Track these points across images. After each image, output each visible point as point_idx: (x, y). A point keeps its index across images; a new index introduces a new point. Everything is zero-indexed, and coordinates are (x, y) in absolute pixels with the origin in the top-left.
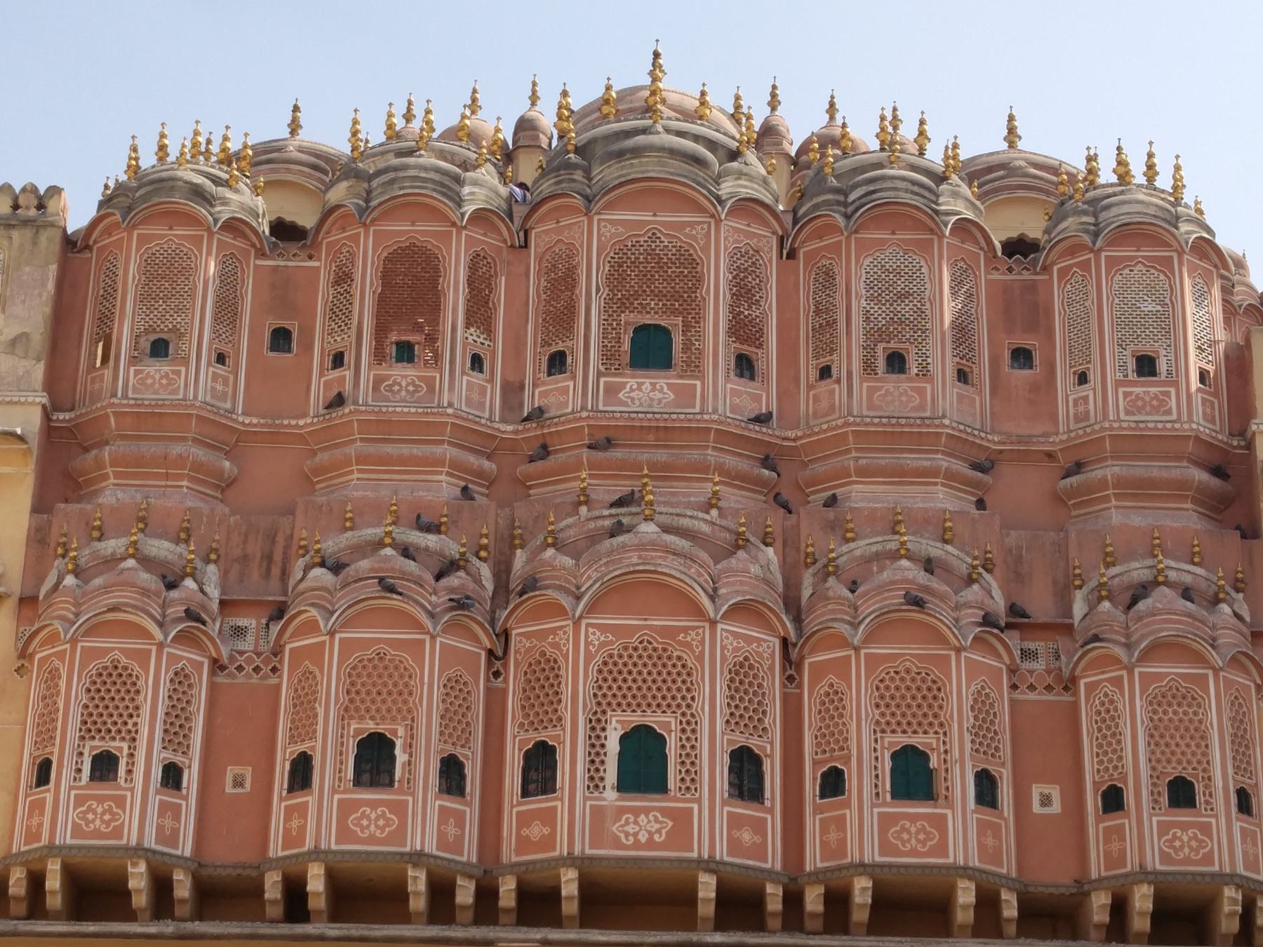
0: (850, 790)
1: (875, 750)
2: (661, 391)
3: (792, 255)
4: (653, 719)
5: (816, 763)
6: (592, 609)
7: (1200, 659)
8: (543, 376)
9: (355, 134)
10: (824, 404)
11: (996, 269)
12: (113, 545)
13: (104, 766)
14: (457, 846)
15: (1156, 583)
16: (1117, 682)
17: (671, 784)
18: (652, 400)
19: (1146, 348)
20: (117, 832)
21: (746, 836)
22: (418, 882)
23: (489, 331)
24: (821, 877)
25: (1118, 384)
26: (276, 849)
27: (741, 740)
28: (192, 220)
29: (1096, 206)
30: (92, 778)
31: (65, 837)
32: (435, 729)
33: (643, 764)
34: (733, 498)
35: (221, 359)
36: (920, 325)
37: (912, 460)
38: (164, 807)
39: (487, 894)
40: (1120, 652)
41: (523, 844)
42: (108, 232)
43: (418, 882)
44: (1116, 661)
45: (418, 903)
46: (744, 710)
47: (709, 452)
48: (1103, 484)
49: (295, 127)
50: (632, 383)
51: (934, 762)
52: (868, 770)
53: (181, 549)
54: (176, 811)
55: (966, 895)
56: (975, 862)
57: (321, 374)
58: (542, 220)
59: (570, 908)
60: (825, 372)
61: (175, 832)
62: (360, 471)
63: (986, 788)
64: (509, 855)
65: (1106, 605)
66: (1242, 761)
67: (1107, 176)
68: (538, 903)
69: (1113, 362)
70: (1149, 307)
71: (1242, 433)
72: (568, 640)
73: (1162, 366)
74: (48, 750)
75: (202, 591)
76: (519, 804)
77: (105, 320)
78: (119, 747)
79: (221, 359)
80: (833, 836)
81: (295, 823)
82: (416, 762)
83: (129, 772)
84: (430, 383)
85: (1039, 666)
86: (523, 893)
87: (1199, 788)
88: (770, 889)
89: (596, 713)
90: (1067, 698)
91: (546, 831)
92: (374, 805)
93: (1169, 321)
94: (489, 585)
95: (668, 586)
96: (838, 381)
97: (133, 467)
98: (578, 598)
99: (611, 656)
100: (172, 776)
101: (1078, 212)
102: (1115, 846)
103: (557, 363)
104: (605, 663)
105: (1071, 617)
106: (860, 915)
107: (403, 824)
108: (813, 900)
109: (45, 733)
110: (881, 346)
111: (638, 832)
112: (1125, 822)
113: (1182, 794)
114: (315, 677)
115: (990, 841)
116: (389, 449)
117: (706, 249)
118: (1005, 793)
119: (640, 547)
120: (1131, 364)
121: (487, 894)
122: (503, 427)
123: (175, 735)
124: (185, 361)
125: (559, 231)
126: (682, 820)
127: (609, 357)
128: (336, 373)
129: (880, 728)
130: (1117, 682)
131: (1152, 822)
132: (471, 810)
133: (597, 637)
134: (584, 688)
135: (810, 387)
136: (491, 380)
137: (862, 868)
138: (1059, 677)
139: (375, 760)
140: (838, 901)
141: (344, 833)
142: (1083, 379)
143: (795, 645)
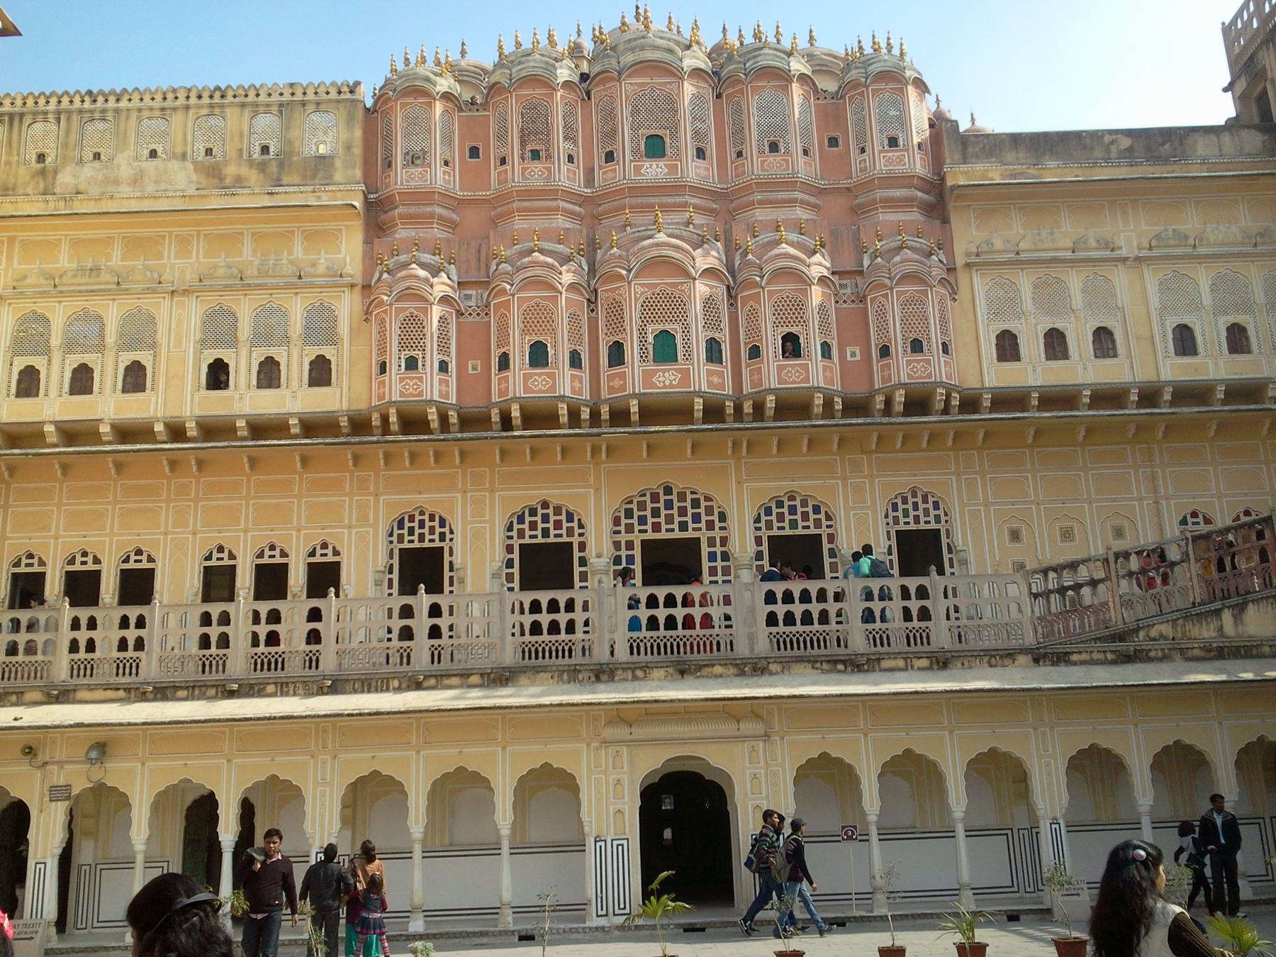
3: (719, 96)
4: (668, 327)
6: (636, 277)
7: (924, 282)
8: (603, 164)
9: (500, 47)
12: (403, 258)
13: (412, 364)
14: (580, 392)
15: (901, 248)
16: (886, 296)
19: (893, 133)
20: (421, 394)
21: (715, 380)
22: (563, 410)
23: (575, 143)
25: (880, 152)
27: (710, 334)
28: (426, 94)
29: (867, 62)
30: (406, 369)
31: (396, 397)
32: (566, 338)
34: (699, 219)
35: (446, 163)
36: (784, 130)
37: (781, 195)
38: (441, 381)
39: (595, 415)
40: (887, 281)
42: (385, 103)
43: (563, 410)
44: (885, 286)
45: (564, 420)
46: (711, 320)
48: (874, 202)
49: (463, 53)
50: (647, 164)
51: (801, 340)
52: (771, 344)
53: (437, 258)
54: (447, 382)
56: (822, 385)
58: (596, 85)
59: (635, 418)
60: (740, 154)
61: (448, 392)
63: (826, 350)
64: (605, 394)
65: (879, 260)
66: (945, 331)
67: (868, 50)
68: (620, 416)
69: (878, 140)
70: (893, 113)
71: (939, 174)
73: (901, 142)
77: (388, 150)
78: (417, 354)
79: (446, 163)
80: (756, 377)
81: (503, 386)
82: (559, 352)
84: (549, 169)
85: (848, 291)
87: (925, 343)
90: (861, 305)
92: (540, 375)
93: (903, 120)
95: (672, 263)
97: (410, 219)
98: (629, 271)
100: (443, 367)
101: (857, 68)
102: (886, 373)
103: (610, 157)
106: (770, 413)
107: (554, 383)
108: (748, 408)
109: (382, 349)
111: (666, 380)
112: (891, 361)
113: (917, 346)
115: (828, 374)
116: (536, 204)
117: (678, 95)
118: (835, 352)
119: (657, 245)
120: (886, 142)
121: (595, 415)
123: (443, 347)
124: (429, 165)
125: (605, 90)
126: (685, 374)
127: (634, 152)
128: (504, 167)
129: (776, 325)
130: (886, 296)
131: (903, 361)
132: (586, 376)
133: (640, 290)
134: (636, 315)
135: (733, 163)
136: (578, 168)
137: (770, 391)
138: (858, 297)
139: (539, 355)
140: (759, 408)
141: (527, 389)
142: (863, 151)
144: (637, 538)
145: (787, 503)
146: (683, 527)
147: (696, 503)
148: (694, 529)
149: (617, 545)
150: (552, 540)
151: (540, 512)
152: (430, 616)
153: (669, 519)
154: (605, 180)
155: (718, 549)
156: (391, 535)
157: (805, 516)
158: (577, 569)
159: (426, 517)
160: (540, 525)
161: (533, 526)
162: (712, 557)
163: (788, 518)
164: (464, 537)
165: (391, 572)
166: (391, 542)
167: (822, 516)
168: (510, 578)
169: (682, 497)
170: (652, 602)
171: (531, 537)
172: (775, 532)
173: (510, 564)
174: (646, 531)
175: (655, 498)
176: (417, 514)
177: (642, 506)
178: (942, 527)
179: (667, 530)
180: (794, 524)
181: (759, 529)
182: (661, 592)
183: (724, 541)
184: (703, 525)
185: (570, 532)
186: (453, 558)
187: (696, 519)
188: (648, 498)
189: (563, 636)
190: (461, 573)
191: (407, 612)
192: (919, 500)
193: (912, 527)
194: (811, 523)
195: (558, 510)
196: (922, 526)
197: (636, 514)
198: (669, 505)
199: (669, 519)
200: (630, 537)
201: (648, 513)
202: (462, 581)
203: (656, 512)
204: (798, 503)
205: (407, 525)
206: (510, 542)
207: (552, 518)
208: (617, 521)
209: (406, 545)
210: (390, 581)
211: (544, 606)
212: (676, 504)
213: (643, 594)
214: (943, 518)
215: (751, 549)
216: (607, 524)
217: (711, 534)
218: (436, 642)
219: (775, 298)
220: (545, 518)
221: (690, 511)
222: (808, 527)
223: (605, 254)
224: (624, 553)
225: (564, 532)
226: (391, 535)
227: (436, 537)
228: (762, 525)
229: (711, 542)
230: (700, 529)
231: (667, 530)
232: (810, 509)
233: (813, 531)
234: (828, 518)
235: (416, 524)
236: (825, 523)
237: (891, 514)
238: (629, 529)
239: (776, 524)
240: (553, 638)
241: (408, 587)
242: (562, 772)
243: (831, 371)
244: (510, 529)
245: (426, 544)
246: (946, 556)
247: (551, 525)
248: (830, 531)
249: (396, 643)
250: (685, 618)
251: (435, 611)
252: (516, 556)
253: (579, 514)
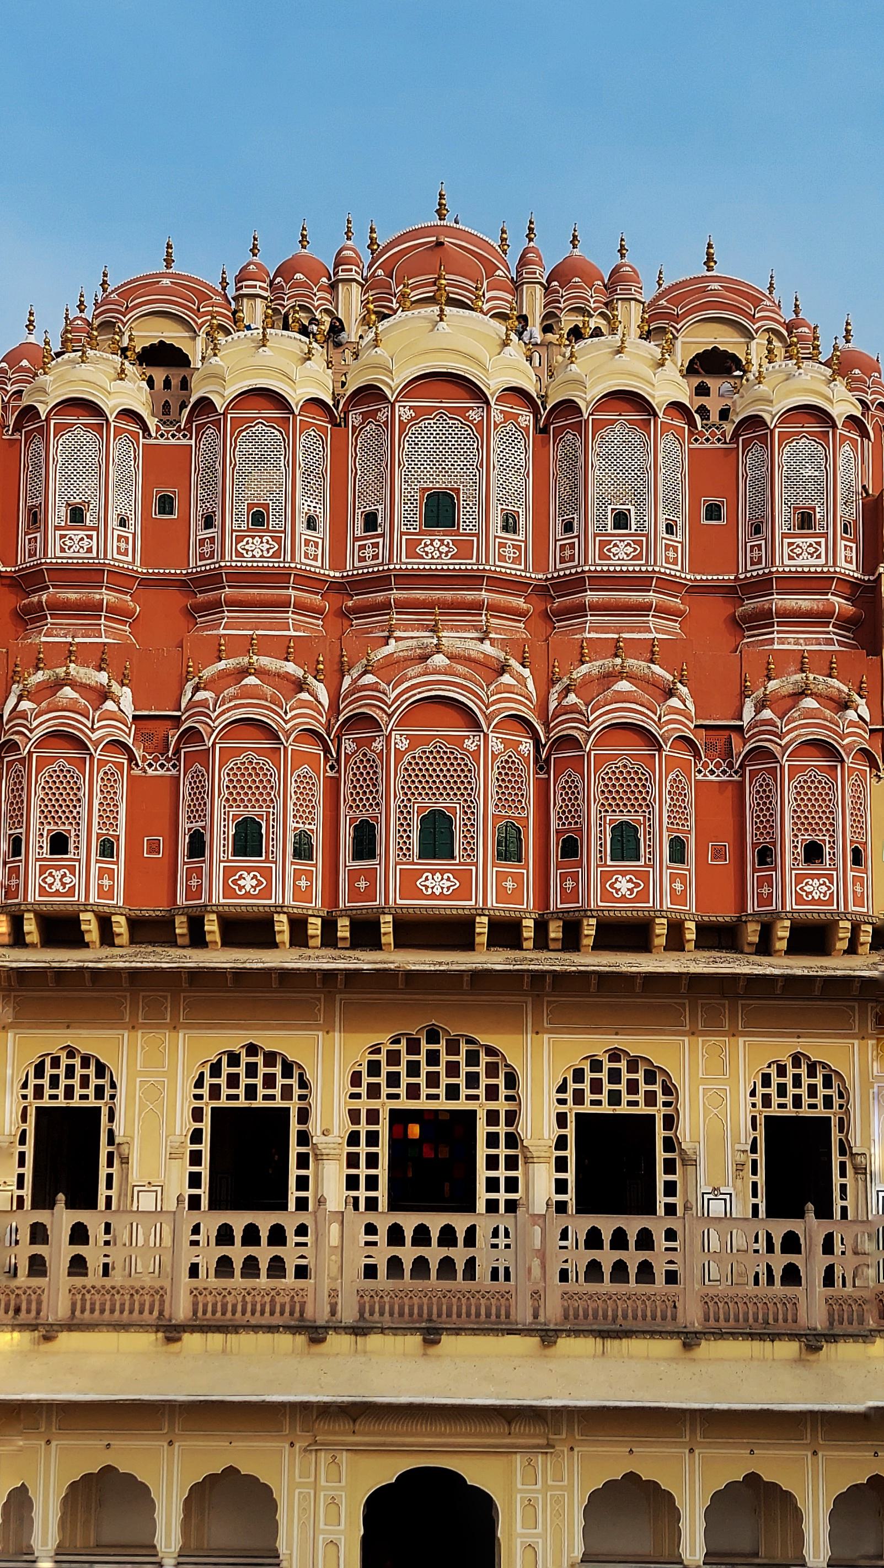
1: (600, 825)
2: (447, 546)
3: (545, 430)
4: (442, 804)
5: (557, 832)
10: (568, 553)
11: (696, 440)
17: (456, 853)
18: (441, 553)
20: (71, 891)
22: (282, 925)
26: (181, 900)
33: (437, 837)
39: (329, 926)
47: (483, 592)
55: (661, 929)
60: (568, 527)
75: (120, 709)
81: (194, 882)
86: (356, 926)
88: (526, 923)
89: (403, 801)
94: (325, 699)
98: (390, 716)
99: (414, 758)
104: (410, 763)
105: (741, 719)
108: (555, 931)
110: (610, 507)
114: (203, 775)
122: (332, 574)
123: (109, 819)
126: (464, 877)
134: (396, 783)
139: (248, 839)
143: (544, 746)
144: (384, 1106)
145: (607, 1065)
146: (453, 1092)
147: (472, 1059)
148: (468, 1097)
149: (354, 1116)
150: (259, 1103)
151: (244, 1059)
152: (71, 1243)
153: (433, 1080)
155: (502, 1129)
156: (25, 1086)
157: (633, 1087)
158: (294, 1150)
159: (77, 1062)
160: (244, 1081)
161: (233, 1081)
162: (492, 1140)
163: (607, 1087)
164: (130, 1097)
165: (22, 1141)
166: (25, 1097)
167: (657, 1088)
168: (196, 1158)
169: (453, 1048)
170: (396, 1236)
171: (229, 1097)
172: (587, 1108)
173: (196, 1137)
174: (397, 1096)
175: (413, 1047)
176: (63, 1055)
177: (394, 1058)
178: (834, 1115)
179: (429, 1097)
180: (615, 1098)
181: (562, 1102)
182: (409, 1222)
183: (512, 1117)
184: (481, 1092)
185: (287, 1093)
186: (114, 1127)
187: (473, 1080)
188: (402, 1046)
189: (263, 1281)
191: (39, 1234)
192: (803, 1071)
193: (790, 1111)
194: (640, 1098)
195: (270, 1059)
196: (805, 1112)
197: (385, 1069)
198: (433, 1058)
199: (433, 1080)
200: (374, 1104)
201: (402, 1069)
202: (125, 1161)
203: (413, 1069)
204: (623, 1065)
205: (49, 1071)
206: (198, 1104)
207: (262, 1070)
208: (356, 1079)
209: (46, 1102)
210: (22, 1155)
211: (238, 1235)
212: (444, 1058)
213: (383, 1221)
214: (836, 1101)
215: (551, 1131)
216: (341, 1086)
217: (492, 1105)
218: (78, 1281)
219: (605, 768)
220: (252, 1070)
221: (464, 1069)
222: (635, 1103)
223: (354, 681)
224: (363, 1128)
225: (277, 1092)
226: (25, 1086)
227: (91, 1091)
228: (569, 1095)
229: (492, 1117)
230: (476, 1098)
231: (429, 1097)
232: (640, 1076)
233: (642, 1109)
234: (667, 1091)
235: (61, 1072)
236: (661, 1098)
237: (760, 1091)
238: (374, 1091)
239: (588, 1096)
240: (250, 1283)
241: (43, 1200)
242: (253, 1479)
243: (683, 882)
244: (199, 1084)
245: (76, 1102)
246: (836, 1159)
247: (259, 1081)
248: (669, 1110)
249: (22, 1279)
250: (442, 1262)
251: (79, 1234)
252: (206, 1126)
253: (300, 1067)
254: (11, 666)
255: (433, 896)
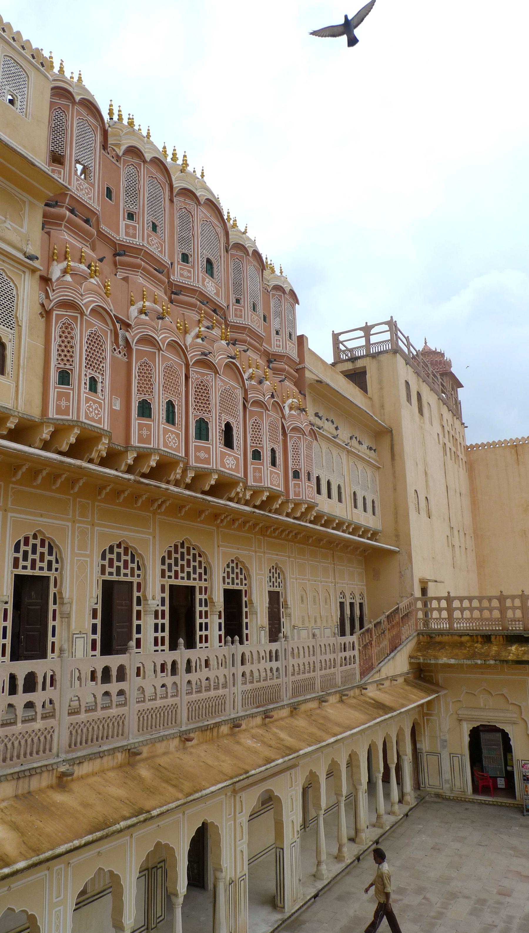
0: (263, 460)
13: (93, 384)
16: (299, 438)
24: (253, 488)
41: (198, 459)
57: (124, 220)
60: (238, 301)
62: (141, 273)
72: (212, 380)
74: (68, 367)
76: (195, 442)
83: (102, 390)
91: (207, 456)
96: (244, 307)
130: (299, 438)
133: (221, 384)
135: (233, 305)
144: (168, 582)
154: (182, 275)
159: (38, 542)
171: (111, 574)
190: (66, 608)
254: (51, 249)
255: (229, 469)
